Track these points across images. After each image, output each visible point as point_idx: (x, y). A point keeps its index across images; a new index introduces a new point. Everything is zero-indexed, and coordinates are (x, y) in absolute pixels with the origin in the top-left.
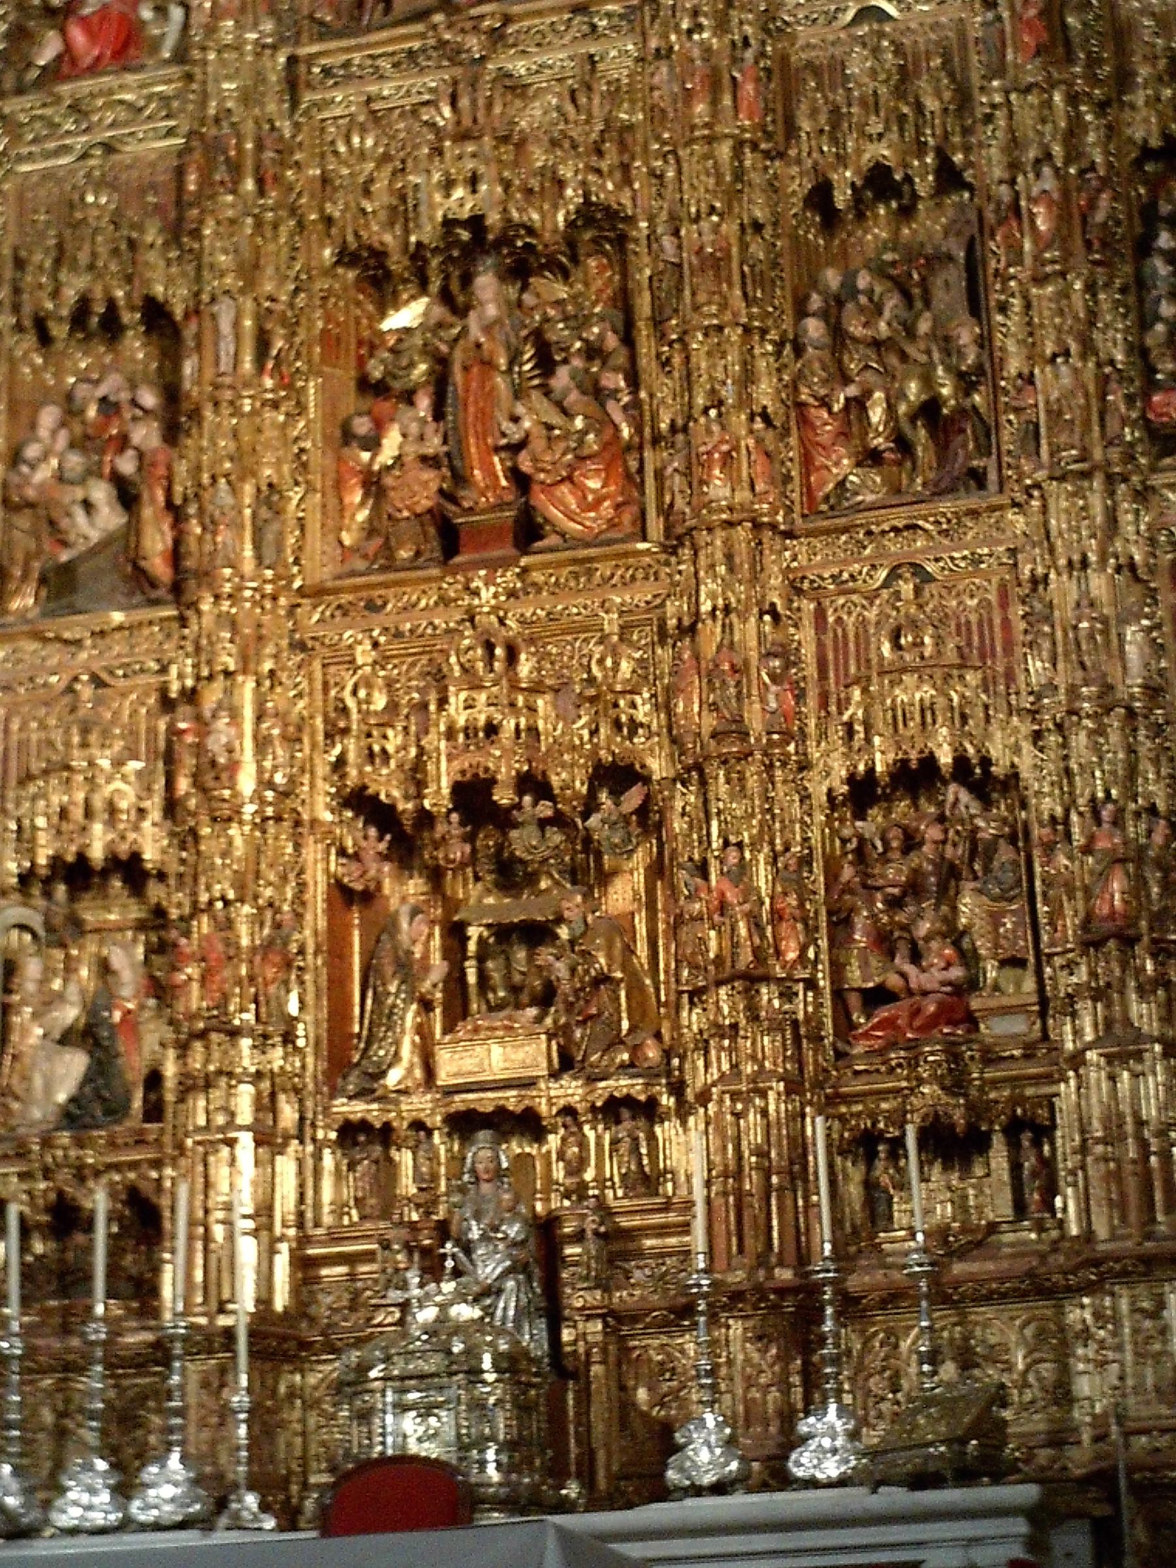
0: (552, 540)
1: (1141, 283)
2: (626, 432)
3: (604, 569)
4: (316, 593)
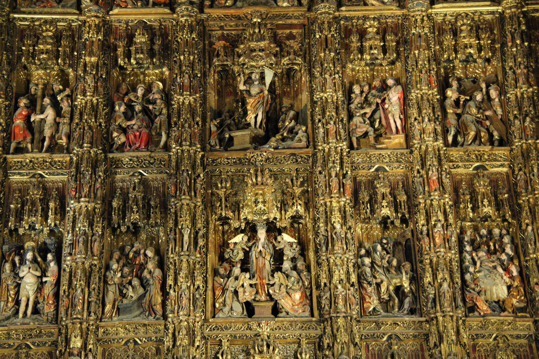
0: (284, 314)
1: (462, 261)
2: (306, 284)
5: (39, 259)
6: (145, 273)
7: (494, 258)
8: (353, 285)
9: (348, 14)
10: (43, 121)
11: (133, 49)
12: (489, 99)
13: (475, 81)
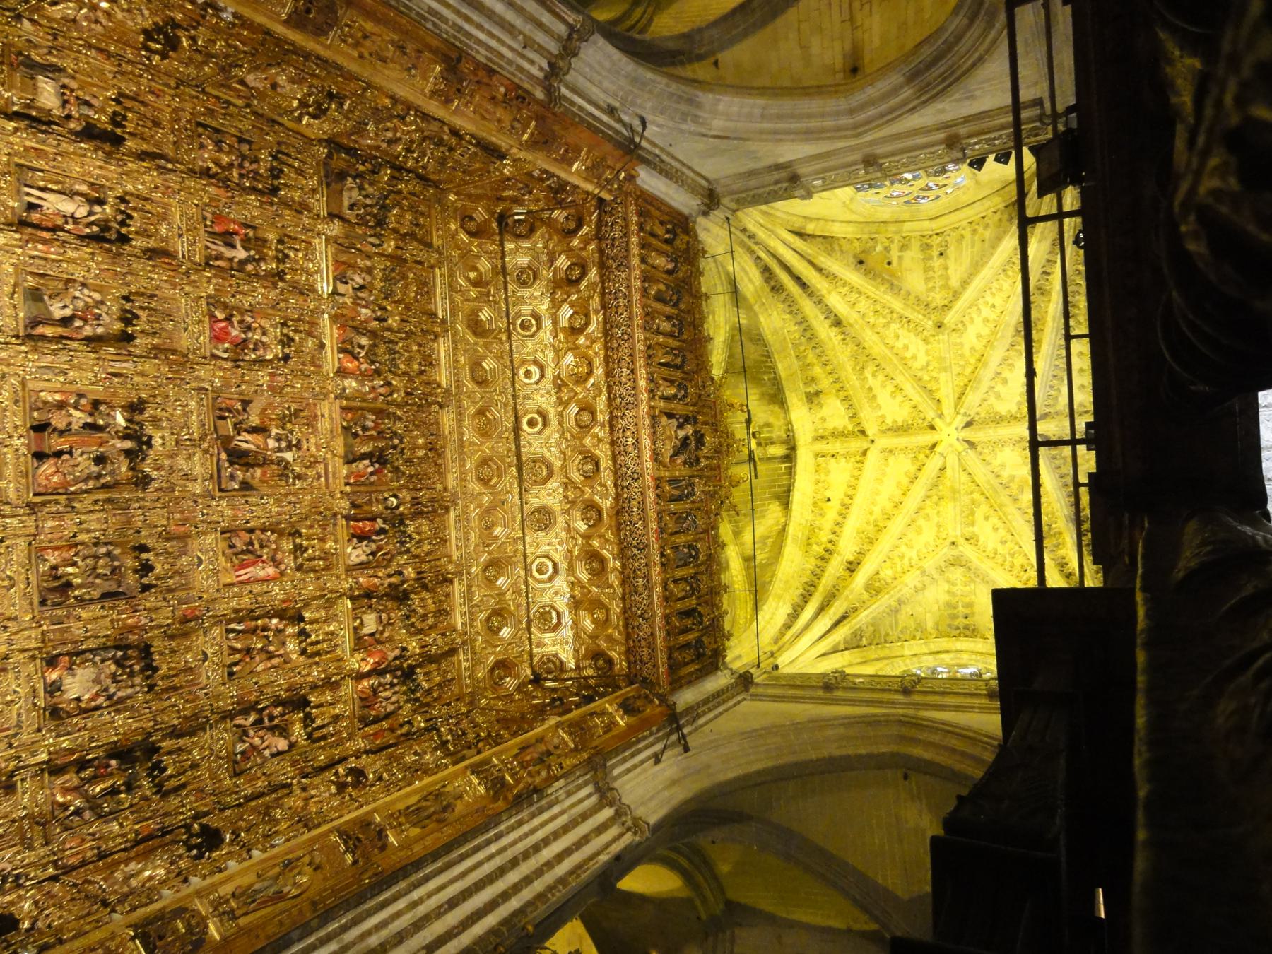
0: (36, 465)
1: (105, 648)
2: (72, 489)
3: (23, 481)
4: (23, 383)
5: (92, 218)
6: (78, 323)
7: (109, 681)
8: (74, 536)
9: (339, 528)
10: (234, 247)
11: (303, 335)
12: (270, 658)
13: (284, 644)
